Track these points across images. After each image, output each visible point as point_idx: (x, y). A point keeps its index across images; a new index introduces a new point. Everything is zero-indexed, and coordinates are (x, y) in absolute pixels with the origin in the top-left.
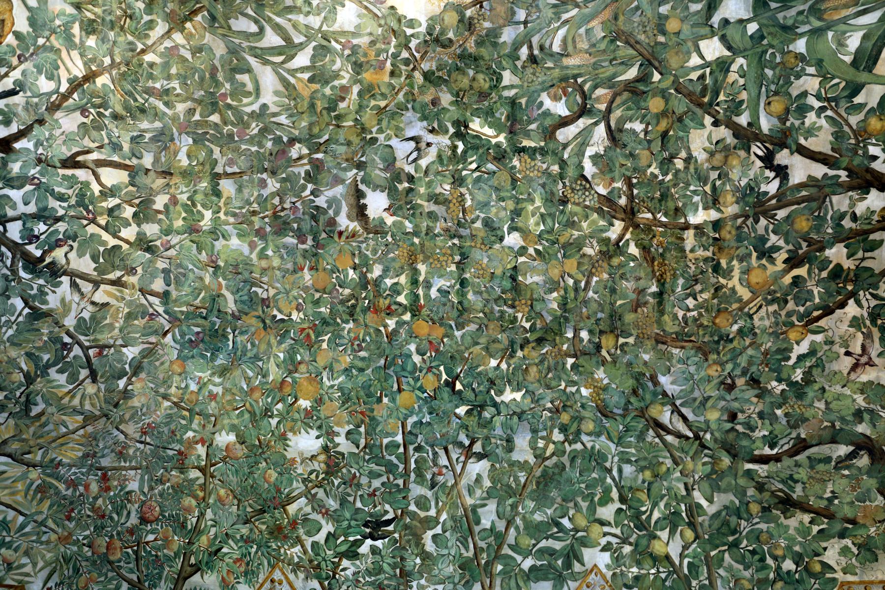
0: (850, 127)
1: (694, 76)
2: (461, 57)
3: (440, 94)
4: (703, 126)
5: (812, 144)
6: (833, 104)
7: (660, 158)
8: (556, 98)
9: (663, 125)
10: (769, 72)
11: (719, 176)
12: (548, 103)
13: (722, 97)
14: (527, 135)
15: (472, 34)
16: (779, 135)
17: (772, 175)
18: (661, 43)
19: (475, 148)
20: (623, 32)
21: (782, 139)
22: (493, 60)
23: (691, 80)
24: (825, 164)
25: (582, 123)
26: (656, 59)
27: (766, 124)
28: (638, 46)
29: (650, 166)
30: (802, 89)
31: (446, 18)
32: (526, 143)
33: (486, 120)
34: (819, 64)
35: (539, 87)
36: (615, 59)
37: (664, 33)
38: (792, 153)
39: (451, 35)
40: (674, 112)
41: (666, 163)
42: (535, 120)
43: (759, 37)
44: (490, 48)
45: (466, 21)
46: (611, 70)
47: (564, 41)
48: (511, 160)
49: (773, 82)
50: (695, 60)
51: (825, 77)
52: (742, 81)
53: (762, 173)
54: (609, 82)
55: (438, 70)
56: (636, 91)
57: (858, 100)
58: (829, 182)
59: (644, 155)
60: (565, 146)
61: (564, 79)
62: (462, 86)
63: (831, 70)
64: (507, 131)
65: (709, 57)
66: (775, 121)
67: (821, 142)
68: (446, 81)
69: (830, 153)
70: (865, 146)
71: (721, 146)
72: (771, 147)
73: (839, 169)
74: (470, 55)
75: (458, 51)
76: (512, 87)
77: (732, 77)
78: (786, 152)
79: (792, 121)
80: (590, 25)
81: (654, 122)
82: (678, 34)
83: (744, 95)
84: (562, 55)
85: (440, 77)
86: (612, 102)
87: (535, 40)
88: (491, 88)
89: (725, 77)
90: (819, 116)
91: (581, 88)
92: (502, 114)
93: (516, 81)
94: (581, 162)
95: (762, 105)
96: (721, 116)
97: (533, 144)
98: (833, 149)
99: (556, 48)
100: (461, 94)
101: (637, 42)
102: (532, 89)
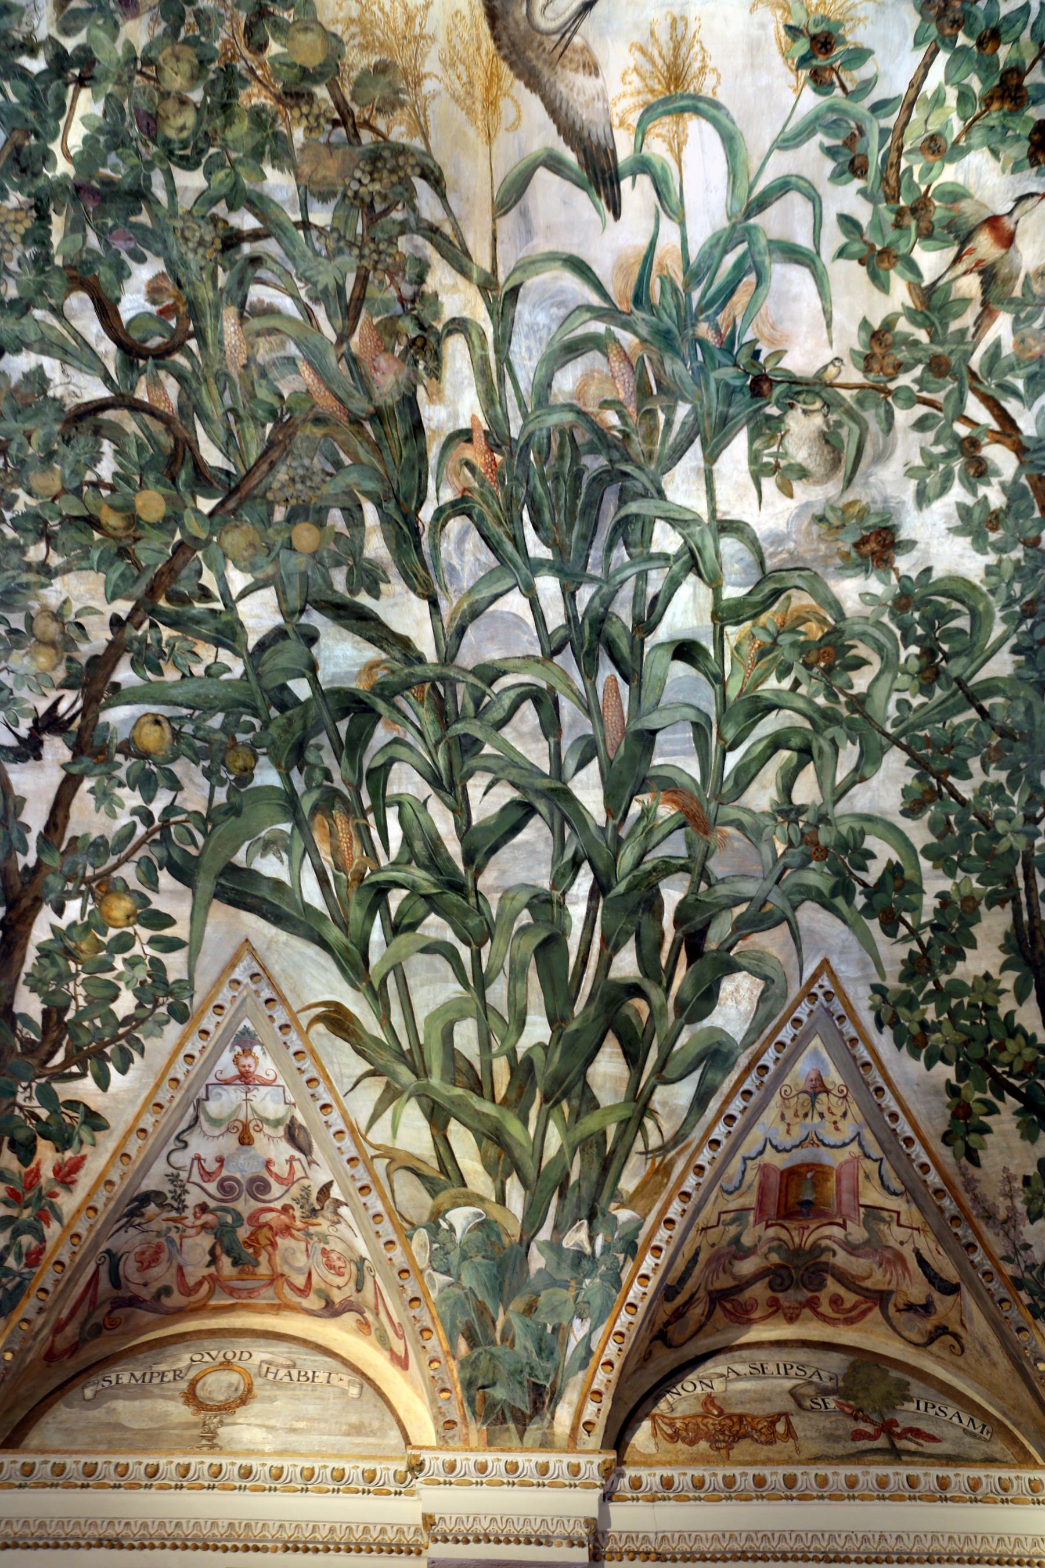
0: (115, 867)
1: (208, 579)
2: (228, 73)
3: (145, 18)
4: (112, 598)
5: (83, 801)
6: (157, 836)
7: (46, 514)
8: (154, 292)
9: (113, 520)
10: (216, 721)
11: (16, 631)
12: (143, 274)
13: (166, 632)
14: (75, 227)
15: (278, 99)
16: (97, 742)
17: (23, 731)
18: (271, 514)
19: (35, 101)
20: (291, 436)
21: (90, 747)
22: (225, 148)
23: (200, 573)
24: (47, 828)
25: (107, 348)
26: (240, 504)
27: (118, 717)
28: (265, 467)
29: (30, 493)
30: (185, 782)
31: (310, 37)
32: (58, 224)
33: (99, 130)
34: (233, 810)
35: (175, 254)
36: (238, 419)
37: (291, 518)
38: (64, 766)
39: (274, 48)
40: (137, 540)
41: (36, 526)
42: (107, 246)
43: (283, 700)
44: (249, 143)
45: (306, 85)
46: (215, 412)
47: (270, 311)
48: (20, 188)
49: (197, 728)
50: (238, 580)
51: (208, 820)
52: (199, 670)
53: (24, 713)
54: (191, 407)
55: (199, 14)
56: (176, 463)
57: (165, 878)
58: (14, 836)
59: (52, 481)
60: (58, 312)
61: (194, 311)
62: (168, 73)
63: (220, 829)
64: (83, 180)
65: (245, 609)
66: (124, 734)
67: (86, 818)
68: (176, 33)
69: (68, 835)
70: (80, 893)
71: (74, 633)
72: (74, 726)
73: (40, 851)
74: (232, 94)
75: (240, 65)
76: (172, 193)
77: (207, 653)
78: (67, 755)
79: (124, 765)
80: (303, 367)
81: (118, 501)
82: (290, 546)
83: (171, 675)
84: (242, 306)
85: (182, 19)
86: (153, 412)
87: (270, 247)
88: (167, 142)
89: (207, 639)
90: (134, 812)
91: (178, 346)
92: (115, 169)
93: (185, 202)
94: (29, 347)
95: (154, 709)
96: (130, 632)
97: (56, 239)
98: (74, 839)
99: (257, 293)
100: (151, 71)
101: (272, 465)
102: (171, 239)
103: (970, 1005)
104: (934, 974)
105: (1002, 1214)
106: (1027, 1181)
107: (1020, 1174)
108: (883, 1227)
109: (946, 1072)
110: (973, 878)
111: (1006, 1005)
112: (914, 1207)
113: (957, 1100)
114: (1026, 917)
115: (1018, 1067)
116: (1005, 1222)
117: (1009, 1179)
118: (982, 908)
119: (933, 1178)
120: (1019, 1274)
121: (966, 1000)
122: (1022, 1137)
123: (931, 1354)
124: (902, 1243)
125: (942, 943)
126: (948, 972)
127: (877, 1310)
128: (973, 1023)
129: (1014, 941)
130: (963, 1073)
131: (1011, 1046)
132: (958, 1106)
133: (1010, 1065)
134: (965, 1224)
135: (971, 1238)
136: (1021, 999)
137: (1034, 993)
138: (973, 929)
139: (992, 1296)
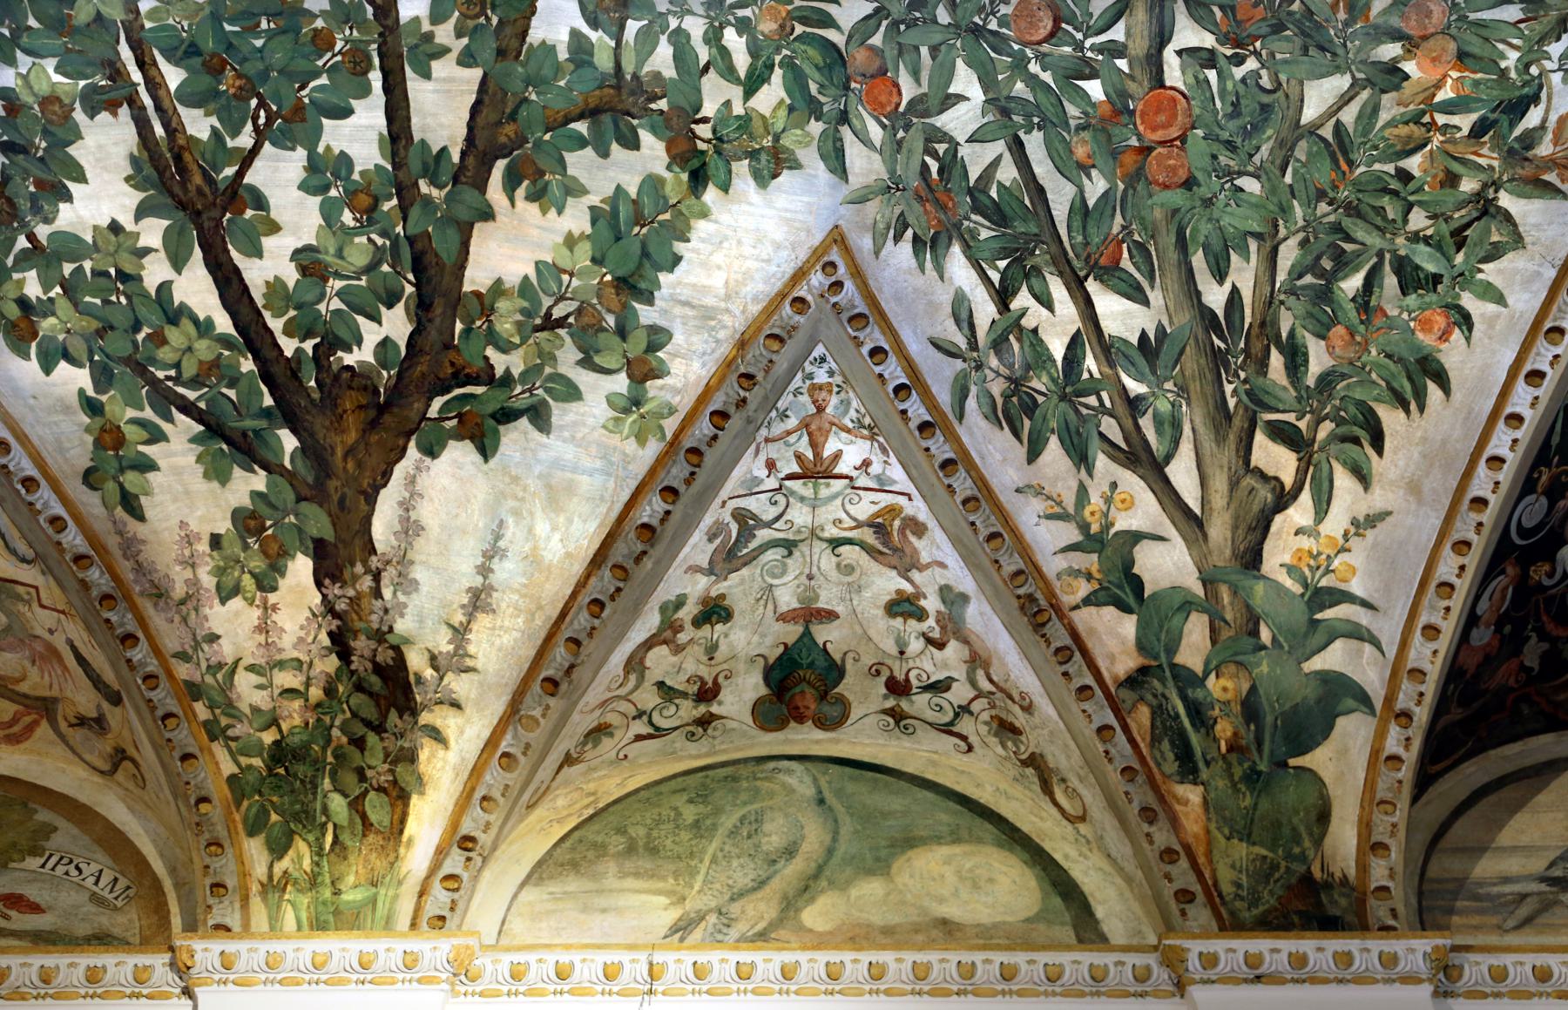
103: (99, 274)
104: (24, 225)
105: (179, 591)
106: (216, 541)
107: (205, 531)
108: (23, 608)
109: (74, 378)
110: (50, 65)
111: (155, 272)
112: (51, 579)
113: (99, 421)
114: (159, 131)
115: (189, 369)
116: (183, 602)
117: (189, 539)
118: (79, 115)
119: (73, 539)
120: (197, 678)
121: (88, 265)
122: (206, 476)
123: (119, 784)
124: (51, 632)
125: (26, 174)
126: (48, 221)
127: (44, 724)
128: (106, 302)
129: (148, 170)
130: (103, 378)
131: (174, 335)
132: (103, 430)
133: (177, 366)
134: (123, 605)
135: (131, 626)
136: (178, 263)
137: (198, 253)
138: (72, 150)
139: (153, 709)
